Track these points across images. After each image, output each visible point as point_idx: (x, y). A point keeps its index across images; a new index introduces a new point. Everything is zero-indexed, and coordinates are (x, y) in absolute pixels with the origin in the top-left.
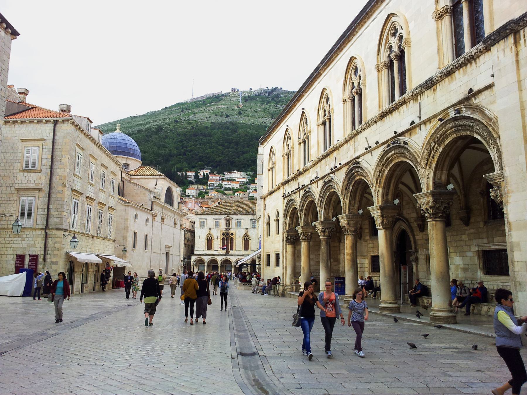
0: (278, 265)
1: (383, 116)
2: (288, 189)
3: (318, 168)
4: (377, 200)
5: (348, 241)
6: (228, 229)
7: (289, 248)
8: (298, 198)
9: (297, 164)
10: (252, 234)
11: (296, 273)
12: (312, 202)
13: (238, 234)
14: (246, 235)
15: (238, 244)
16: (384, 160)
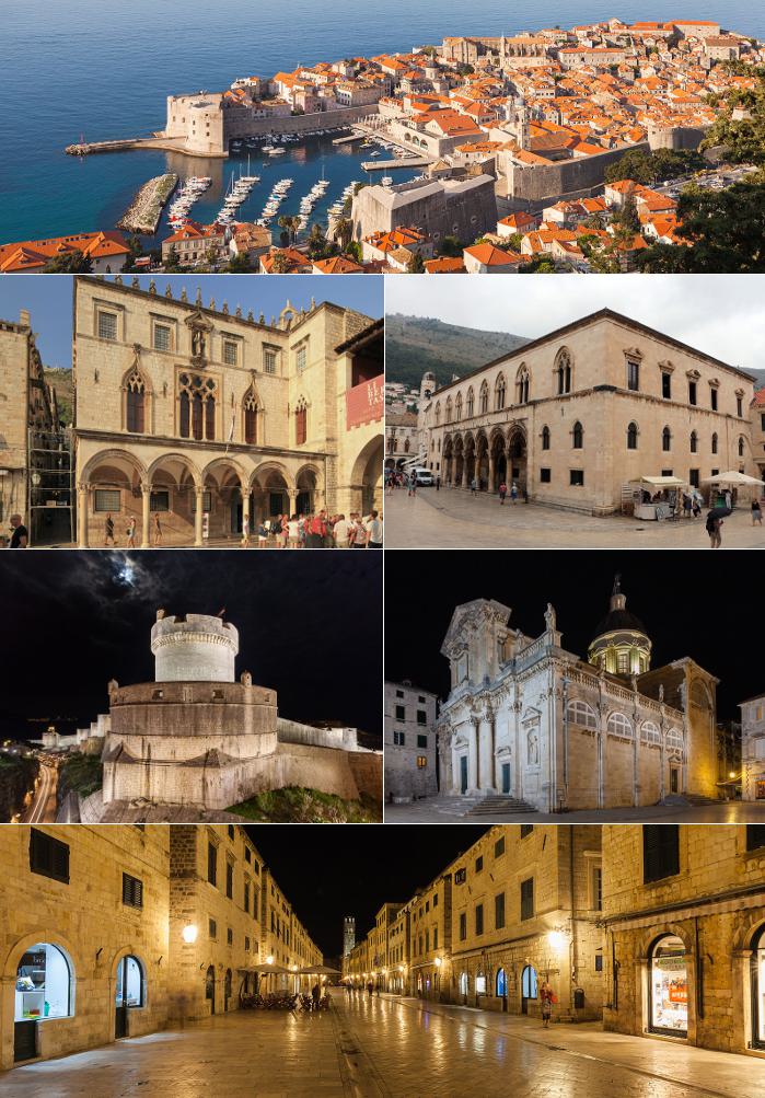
0: (438, 469)
1: (495, 413)
2: (448, 429)
3: (465, 423)
4: (490, 448)
5: (477, 463)
6: (393, 436)
7: (446, 461)
8: (453, 436)
9: (454, 418)
10: (412, 440)
11: (449, 474)
12: (460, 439)
13: (401, 440)
14: (407, 440)
15: (400, 447)
16: (494, 430)
